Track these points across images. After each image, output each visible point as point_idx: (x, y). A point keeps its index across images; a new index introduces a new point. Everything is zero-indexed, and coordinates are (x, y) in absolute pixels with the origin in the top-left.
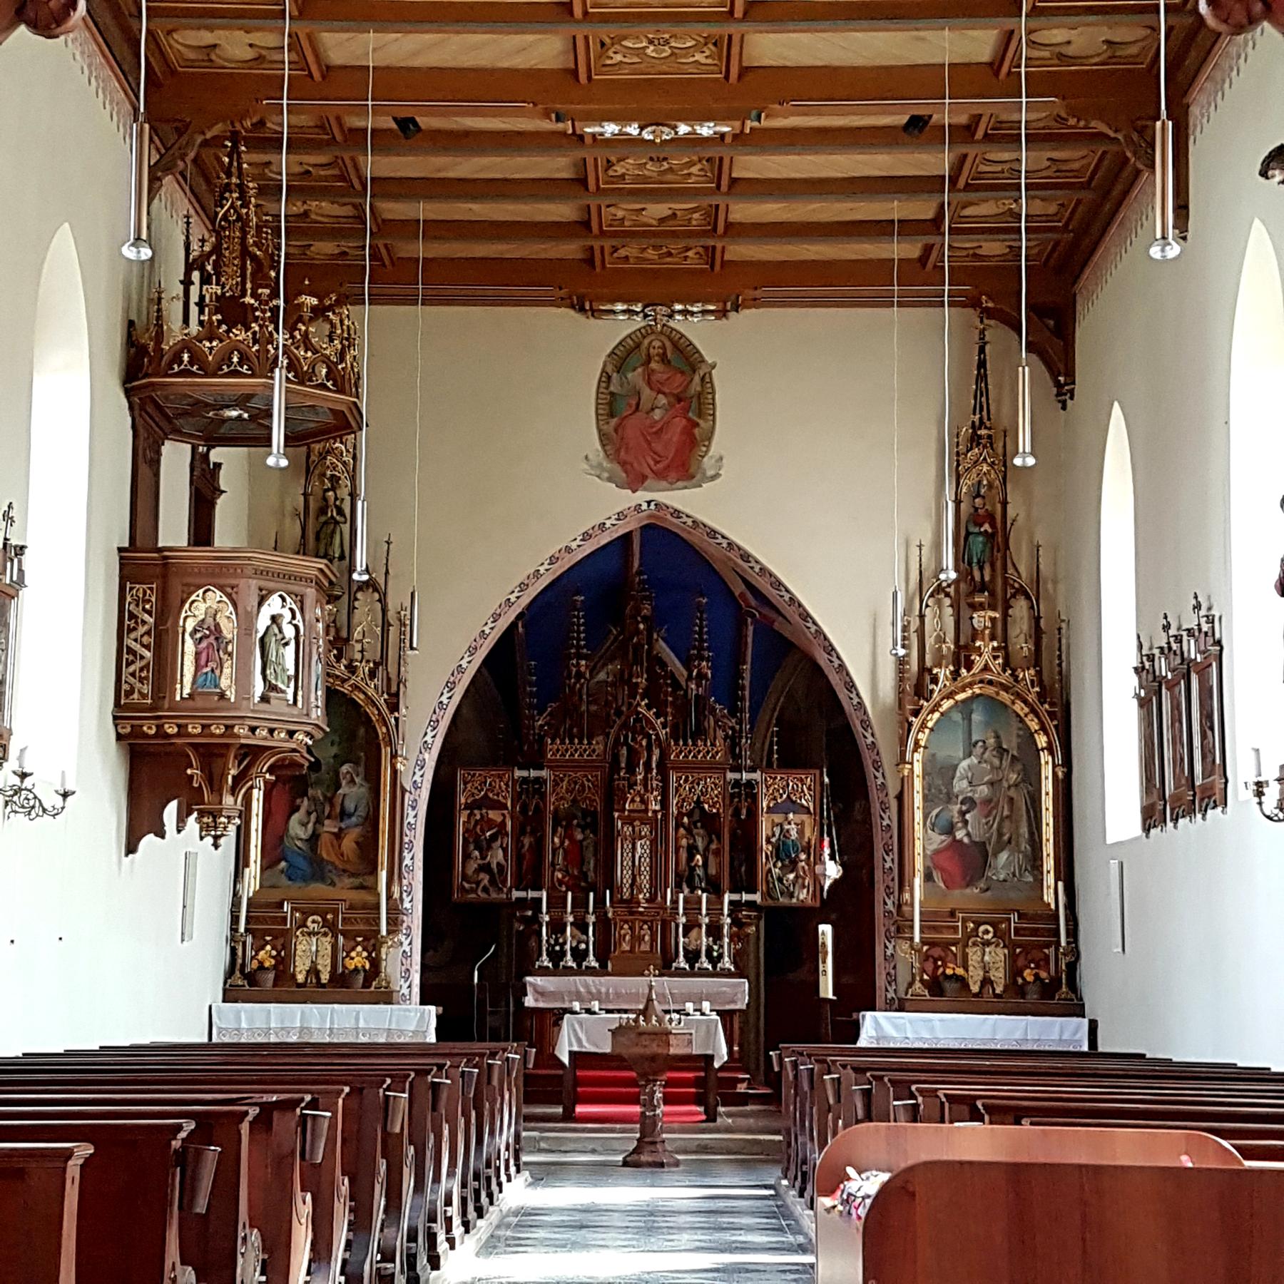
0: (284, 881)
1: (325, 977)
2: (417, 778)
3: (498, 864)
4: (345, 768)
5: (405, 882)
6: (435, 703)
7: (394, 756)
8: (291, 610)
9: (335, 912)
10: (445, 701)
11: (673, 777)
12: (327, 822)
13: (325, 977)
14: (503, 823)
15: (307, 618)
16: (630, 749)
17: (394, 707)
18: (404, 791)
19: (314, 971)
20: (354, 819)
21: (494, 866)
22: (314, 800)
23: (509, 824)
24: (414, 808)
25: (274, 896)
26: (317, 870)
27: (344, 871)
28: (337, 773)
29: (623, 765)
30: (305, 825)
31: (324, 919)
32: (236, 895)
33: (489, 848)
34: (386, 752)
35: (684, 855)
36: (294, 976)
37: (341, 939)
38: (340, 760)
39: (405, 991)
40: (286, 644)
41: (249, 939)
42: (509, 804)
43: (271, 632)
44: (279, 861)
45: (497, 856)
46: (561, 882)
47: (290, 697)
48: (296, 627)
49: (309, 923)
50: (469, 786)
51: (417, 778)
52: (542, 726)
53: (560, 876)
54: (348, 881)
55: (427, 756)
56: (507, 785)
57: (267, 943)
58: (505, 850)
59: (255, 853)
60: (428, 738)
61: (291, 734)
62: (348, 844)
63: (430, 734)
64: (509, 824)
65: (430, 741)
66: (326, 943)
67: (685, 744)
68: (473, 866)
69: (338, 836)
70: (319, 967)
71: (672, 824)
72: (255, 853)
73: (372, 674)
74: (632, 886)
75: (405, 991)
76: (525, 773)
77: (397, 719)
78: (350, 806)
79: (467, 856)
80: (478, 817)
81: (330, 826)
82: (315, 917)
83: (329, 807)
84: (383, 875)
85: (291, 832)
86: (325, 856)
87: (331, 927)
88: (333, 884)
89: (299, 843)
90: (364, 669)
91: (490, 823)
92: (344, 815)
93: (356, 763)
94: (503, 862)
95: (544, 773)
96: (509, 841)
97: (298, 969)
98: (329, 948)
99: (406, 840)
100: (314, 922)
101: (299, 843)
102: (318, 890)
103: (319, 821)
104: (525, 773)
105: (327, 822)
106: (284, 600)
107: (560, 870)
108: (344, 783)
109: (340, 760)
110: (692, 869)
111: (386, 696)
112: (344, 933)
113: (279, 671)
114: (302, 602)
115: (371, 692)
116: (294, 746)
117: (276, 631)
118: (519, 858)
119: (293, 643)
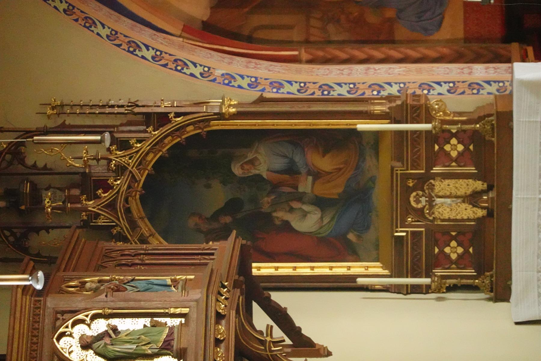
0: (371, 235)
1: (479, 185)
2: (244, 83)
4: (237, 170)
5: (368, 94)
6: (155, 67)
7: (220, 116)
8: (74, 324)
9: (405, 177)
10: (152, 52)
12: (301, 189)
13: (479, 185)
15: (82, 305)
17: (163, 119)
18: (262, 100)
19: (473, 199)
20: (298, 159)
22: (275, 205)
24: (281, 85)
25: (387, 248)
26: (356, 198)
27: (357, 167)
28: (243, 181)
30: (305, 214)
31: (414, 189)
32: (386, 289)
34: (217, 125)
36: (479, 220)
37: (437, 169)
38: (228, 178)
39: (493, 89)
40: (115, 330)
41: (439, 272)
43: (100, 350)
44: (349, 242)
47: (176, 322)
48: (95, 317)
49: (420, 206)
51: (244, 83)
54: (369, 162)
55: (218, 72)
57: (442, 252)
59: (340, 269)
60: (197, 71)
61: (219, 317)
62: (325, 163)
63: (192, 69)
65: (200, 69)
66: (441, 186)
69: (317, 175)
70: (469, 192)
72: (340, 269)
73: (124, 145)
75: (493, 89)
77: (178, 115)
78: (279, 163)
81: (306, 185)
82: (412, 199)
83: (284, 187)
84: (363, 126)
85: (313, 230)
86: (340, 190)
87: (423, 181)
88: (373, 180)
89: (326, 220)
90: (119, 157)
92: (291, 170)
93: (230, 158)
97: (472, 216)
98: (447, 182)
99: (318, 94)
100: (418, 201)
101: (326, 220)
102: (380, 196)
103: (300, 198)
105: (301, 189)
106: (63, 335)
108: (254, 172)
109: (228, 178)
111: (150, 129)
112: (429, 167)
113: (148, 339)
114: (63, 313)
115: (145, 146)
116: (233, 313)
117: (102, 343)
119: (115, 322)
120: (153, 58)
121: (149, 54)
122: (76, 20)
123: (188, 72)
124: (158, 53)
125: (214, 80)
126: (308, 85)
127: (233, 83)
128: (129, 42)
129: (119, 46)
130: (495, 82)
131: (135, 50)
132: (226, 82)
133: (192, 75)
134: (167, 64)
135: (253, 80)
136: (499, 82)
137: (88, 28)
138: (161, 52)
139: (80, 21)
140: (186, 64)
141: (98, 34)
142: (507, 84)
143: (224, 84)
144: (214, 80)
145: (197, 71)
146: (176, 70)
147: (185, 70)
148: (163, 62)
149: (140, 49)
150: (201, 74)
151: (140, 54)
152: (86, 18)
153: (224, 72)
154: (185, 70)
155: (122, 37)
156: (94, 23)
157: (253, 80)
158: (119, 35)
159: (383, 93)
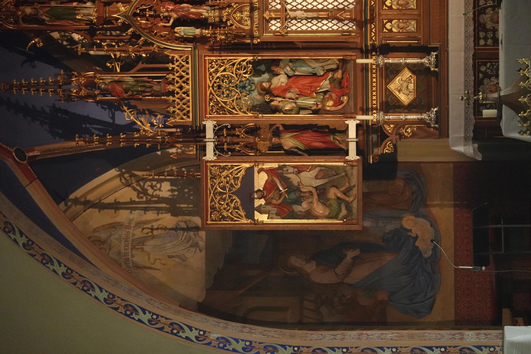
3: (316, 177)
10: (148, 316)
14: (270, 171)
16: (179, 22)
21: (319, 182)
23: (267, 166)
29: (198, 31)
33: (298, 189)
42: (247, 165)
45: (308, 180)
46: (338, 102)
50: (225, 214)
52: (152, 125)
53: (331, 103)
55: (214, 336)
56: (224, 168)
58: (299, 170)
60: (192, 335)
63: (188, 333)
64: (267, 166)
65: (195, 333)
68: (319, 209)
74: (340, 20)
76: (210, 147)
79: (308, 215)
80: (263, 202)
91: (270, 186)
94: (314, 173)
95: (210, 125)
96: (292, 163)
104: (210, 147)
107: (323, 101)
118: (311, 152)
120: (149, 321)
121: (145, 318)
122: (75, 284)
123: (184, 335)
124: (155, 317)
125: (209, 344)
126: (301, 349)
127: (228, 347)
128: (126, 305)
129: (116, 309)
130: (486, 347)
131: (131, 314)
132: (221, 345)
133: (187, 338)
134: (163, 328)
135: (248, 343)
136: (490, 347)
137: (85, 291)
138: (158, 316)
139: (78, 284)
140: (181, 328)
141: (96, 297)
142: (498, 349)
143: (219, 347)
144: (209, 344)
145: (192, 335)
146: (172, 333)
147: (181, 334)
148: (159, 326)
149: (137, 313)
150: (197, 338)
151: (136, 317)
152: (84, 281)
153: (219, 336)
154: (181, 334)
155: (119, 301)
156: (92, 286)
157: (248, 343)
158: (116, 298)
159: (372, 30)
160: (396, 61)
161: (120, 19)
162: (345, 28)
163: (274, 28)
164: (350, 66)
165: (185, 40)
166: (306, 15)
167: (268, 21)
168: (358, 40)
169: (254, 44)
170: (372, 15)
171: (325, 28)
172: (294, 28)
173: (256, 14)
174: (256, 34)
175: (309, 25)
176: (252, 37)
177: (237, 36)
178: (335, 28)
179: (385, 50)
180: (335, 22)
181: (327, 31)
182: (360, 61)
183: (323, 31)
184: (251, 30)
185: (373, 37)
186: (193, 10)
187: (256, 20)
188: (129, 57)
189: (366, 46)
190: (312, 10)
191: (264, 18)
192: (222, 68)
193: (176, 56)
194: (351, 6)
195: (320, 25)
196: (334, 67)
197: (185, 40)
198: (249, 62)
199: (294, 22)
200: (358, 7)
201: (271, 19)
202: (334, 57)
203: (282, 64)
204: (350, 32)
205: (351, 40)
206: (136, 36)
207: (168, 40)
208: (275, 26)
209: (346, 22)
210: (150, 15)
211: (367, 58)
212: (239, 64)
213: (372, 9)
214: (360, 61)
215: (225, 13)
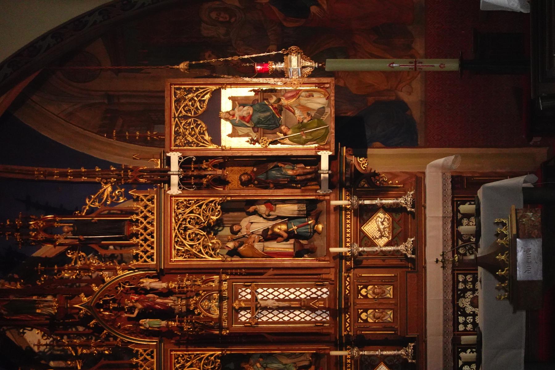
11: (177, 260)
16: (144, 314)
29: (164, 323)
35: (274, 246)
67: (136, 245)
71: (236, 261)
74: (313, 310)
110: (291, 235)
160: (372, 353)
161: (82, 309)
162: (319, 319)
163: (243, 319)
164: (324, 360)
165: (149, 333)
166: (277, 304)
167: (238, 311)
168: (332, 331)
169: (222, 336)
170: (346, 303)
171: (297, 319)
172: (265, 319)
173: (225, 303)
174: (225, 324)
175: (281, 315)
176: (221, 328)
177: (205, 327)
178: (308, 318)
179: (361, 342)
180: (307, 312)
181: (299, 322)
182: (333, 353)
183: (295, 322)
184: (220, 319)
185: (347, 326)
186: (159, 300)
187: (225, 311)
188: (92, 353)
189: (341, 336)
190: (283, 300)
191: (234, 308)
192: (189, 364)
193: (141, 350)
194: (325, 296)
195: (292, 315)
196: (306, 363)
197: (149, 333)
198: (217, 357)
199: (265, 312)
200: (332, 295)
201: (242, 309)
202: (308, 350)
203: (252, 361)
204: (324, 323)
205: (324, 331)
206: (98, 330)
207: (131, 333)
208: (245, 316)
209: (319, 312)
210: (114, 308)
211: (341, 350)
212: (207, 358)
213: (347, 298)
214: (333, 353)
215: (192, 302)
